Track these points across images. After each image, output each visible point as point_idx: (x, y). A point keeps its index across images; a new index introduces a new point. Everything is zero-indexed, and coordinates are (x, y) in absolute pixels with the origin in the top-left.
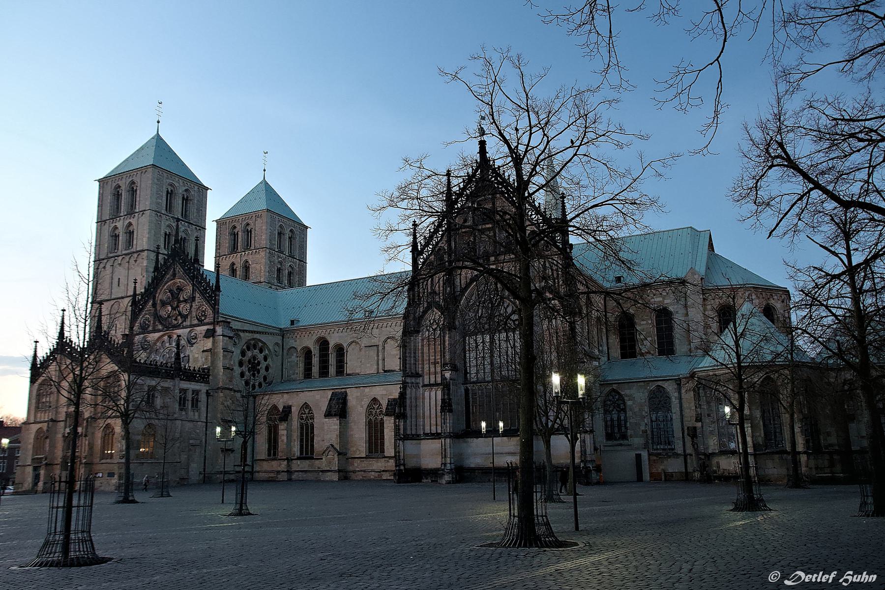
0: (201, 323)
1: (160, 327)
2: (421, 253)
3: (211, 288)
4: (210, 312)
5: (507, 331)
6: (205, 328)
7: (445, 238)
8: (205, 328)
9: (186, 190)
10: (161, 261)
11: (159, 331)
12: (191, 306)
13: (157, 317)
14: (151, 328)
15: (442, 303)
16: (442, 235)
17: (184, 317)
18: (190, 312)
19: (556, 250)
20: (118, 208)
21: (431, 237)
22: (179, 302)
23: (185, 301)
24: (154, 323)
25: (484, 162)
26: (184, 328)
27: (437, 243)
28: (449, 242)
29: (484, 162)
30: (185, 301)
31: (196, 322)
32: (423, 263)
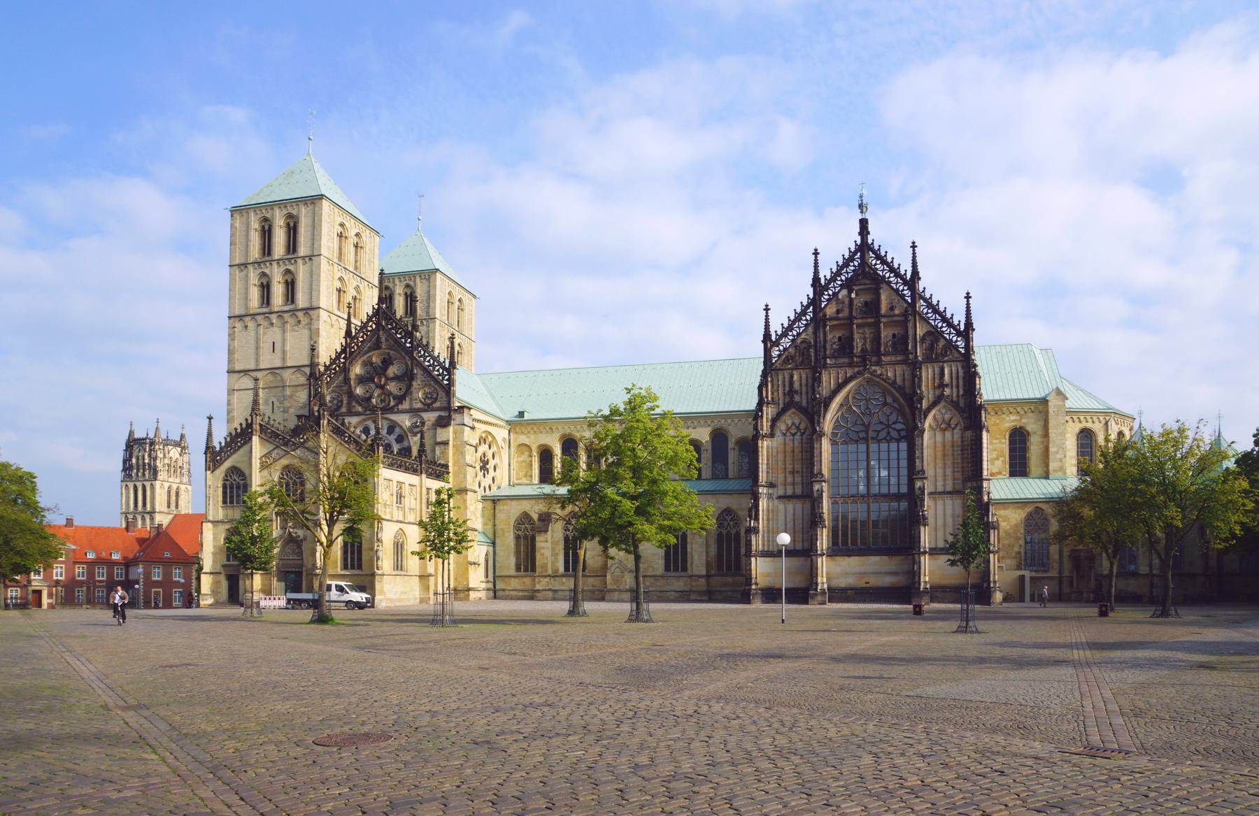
0: (428, 408)
1: (360, 409)
2: (777, 343)
3: (442, 365)
4: (442, 394)
5: (888, 442)
6: (436, 414)
7: (810, 330)
8: (436, 414)
9: (357, 235)
10: (356, 322)
11: (358, 414)
12: (409, 386)
13: (350, 394)
14: (344, 410)
15: (804, 403)
16: (806, 325)
17: (400, 399)
18: (408, 391)
19: (956, 355)
20: (267, 248)
21: (790, 328)
22: (387, 379)
23: (397, 378)
24: (349, 404)
25: (864, 247)
26: (399, 412)
27: (799, 334)
28: (815, 333)
29: (864, 247)
30: (397, 378)
31: (419, 405)
32: (779, 356)
